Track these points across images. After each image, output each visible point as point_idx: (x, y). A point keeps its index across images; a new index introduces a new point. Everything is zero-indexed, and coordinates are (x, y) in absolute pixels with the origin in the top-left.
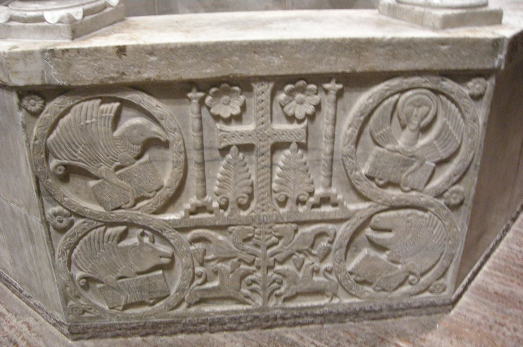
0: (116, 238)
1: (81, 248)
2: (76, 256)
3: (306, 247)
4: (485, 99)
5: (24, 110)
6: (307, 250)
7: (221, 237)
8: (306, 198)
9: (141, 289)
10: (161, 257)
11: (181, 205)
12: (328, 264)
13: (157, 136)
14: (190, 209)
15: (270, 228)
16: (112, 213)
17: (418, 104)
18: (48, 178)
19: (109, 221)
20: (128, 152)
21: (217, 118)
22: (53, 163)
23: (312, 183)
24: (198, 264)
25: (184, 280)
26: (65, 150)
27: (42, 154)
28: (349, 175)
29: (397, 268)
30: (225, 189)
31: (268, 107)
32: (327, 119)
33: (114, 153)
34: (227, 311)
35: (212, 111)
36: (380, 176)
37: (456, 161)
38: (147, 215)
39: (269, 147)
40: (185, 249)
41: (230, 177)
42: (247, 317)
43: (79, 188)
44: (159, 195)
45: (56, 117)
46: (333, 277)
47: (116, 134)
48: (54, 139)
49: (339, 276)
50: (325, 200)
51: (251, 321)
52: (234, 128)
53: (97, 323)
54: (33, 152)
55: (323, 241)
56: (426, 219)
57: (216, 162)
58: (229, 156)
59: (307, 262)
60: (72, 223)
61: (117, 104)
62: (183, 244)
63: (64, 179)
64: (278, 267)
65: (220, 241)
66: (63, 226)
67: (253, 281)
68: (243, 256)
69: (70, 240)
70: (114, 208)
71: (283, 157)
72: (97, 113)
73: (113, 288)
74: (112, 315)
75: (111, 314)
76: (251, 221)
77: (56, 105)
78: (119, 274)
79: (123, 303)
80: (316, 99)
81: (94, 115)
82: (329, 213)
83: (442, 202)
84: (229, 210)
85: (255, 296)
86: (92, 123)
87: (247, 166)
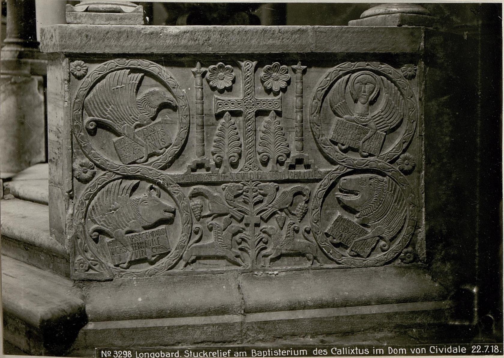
0: (129, 191)
1: (98, 199)
2: (93, 207)
3: (287, 206)
6: (287, 208)
10: (165, 211)
13: (169, 101)
16: (129, 167)
17: (365, 82)
18: (81, 132)
19: (126, 174)
21: (213, 89)
26: (98, 109)
28: (317, 139)
29: (367, 233)
35: (211, 83)
36: (342, 141)
39: (254, 113)
40: (186, 203)
43: (104, 144)
47: (139, 97)
50: (299, 161)
54: (73, 108)
58: (222, 121)
59: (288, 222)
61: (142, 74)
64: (263, 226)
66: (86, 177)
69: (90, 191)
71: (264, 123)
78: (127, 229)
79: (128, 260)
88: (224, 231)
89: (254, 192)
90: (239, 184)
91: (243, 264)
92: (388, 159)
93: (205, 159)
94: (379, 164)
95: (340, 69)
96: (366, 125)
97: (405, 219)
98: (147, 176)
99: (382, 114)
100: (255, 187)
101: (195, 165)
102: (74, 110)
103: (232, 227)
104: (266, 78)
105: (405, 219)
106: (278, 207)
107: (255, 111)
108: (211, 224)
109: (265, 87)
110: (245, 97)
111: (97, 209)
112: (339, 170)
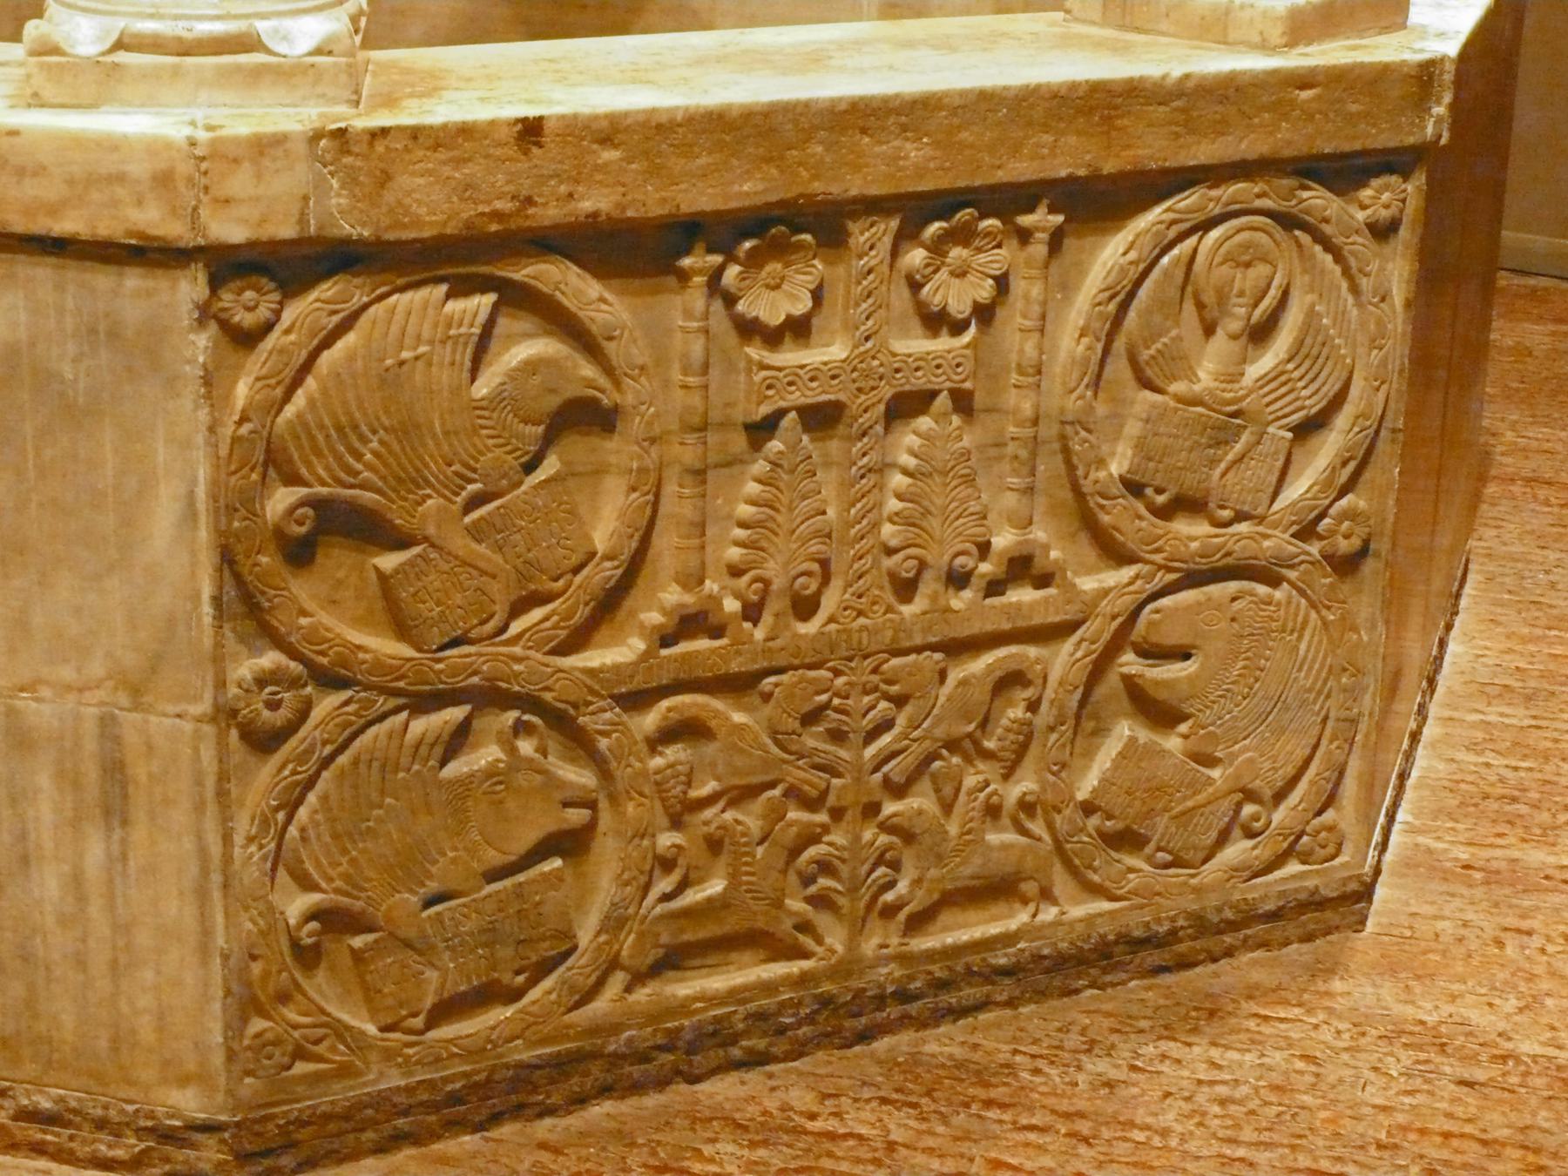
0: (439, 751)
1: (324, 798)
2: (303, 830)
4: (1404, 232)
5: (213, 327)
6: (970, 735)
7: (738, 717)
8: (971, 564)
9: (490, 935)
10: (566, 805)
11: (632, 614)
12: (1024, 785)
14: (662, 625)
15: (875, 671)
16: (439, 661)
17: (1246, 258)
19: (427, 688)
20: (509, 448)
21: (748, 329)
22: (280, 500)
24: (665, 822)
25: (627, 883)
27: (252, 469)
28: (1082, 482)
29: (1210, 781)
30: (762, 549)
33: (465, 450)
34: (745, 988)
35: (741, 307)
37: (1342, 420)
38: (539, 656)
39: (882, 407)
41: (777, 510)
42: (800, 1004)
44: (579, 587)
45: (315, 342)
46: (1037, 827)
47: (481, 389)
48: (299, 415)
49: (1058, 819)
50: (1022, 568)
51: (810, 1019)
52: (790, 356)
53: (339, 1095)
56: (1279, 604)
57: (736, 469)
58: (775, 445)
59: (970, 781)
60: (303, 714)
63: (299, 553)
64: (890, 808)
65: (741, 728)
66: (279, 723)
67: (825, 867)
68: (802, 774)
69: (294, 772)
70: (446, 640)
71: (911, 440)
72: (436, 325)
73: (408, 944)
74: (389, 1055)
75: (386, 1049)
76: (827, 652)
77: (318, 305)
78: (433, 886)
79: (429, 1001)
80: (998, 258)
81: (426, 334)
82: (1033, 605)
83: (1314, 549)
84: (767, 618)
85: (823, 920)
86: (417, 358)
88: (761, 843)
91: (819, 950)
92: (1293, 523)
94: (1266, 543)
95: (1172, 216)
96: (1234, 415)
97: (1326, 718)
98: (504, 685)
99: (1290, 366)
102: (233, 468)
103: (790, 824)
104: (931, 269)
105: (1326, 718)
107: (889, 395)
108: (718, 828)
110: (856, 347)
111: (319, 836)
112: (1139, 582)
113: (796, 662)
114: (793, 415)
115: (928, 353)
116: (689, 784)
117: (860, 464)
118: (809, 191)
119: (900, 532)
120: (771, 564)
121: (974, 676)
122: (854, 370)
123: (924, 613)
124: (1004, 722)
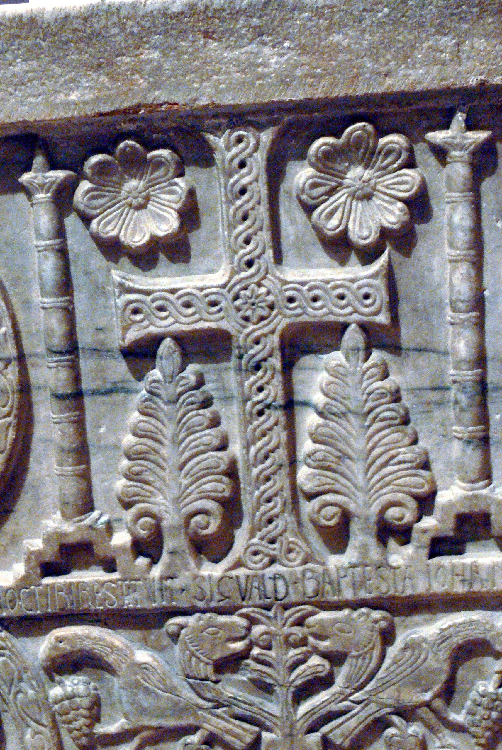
6: (428, 705)
8: (408, 517)
11: (15, 540)
14: (39, 553)
15: (300, 622)
23: (426, 466)
31: (263, 211)
32: (451, 246)
35: (94, 224)
39: (276, 339)
40: (31, 692)
55: (482, 675)
57: (119, 397)
62: (25, 676)
65: (143, 667)
71: (323, 377)
84: (165, 557)
87: (216, 407)
89: (295, 646)
90: (235, 619)
93: (91, 527)
100: (295, 629)
101: (56, 548)
104: (322, 190)
106: (390, 702)
107: (280, 328)
109: (318, 230)
110: (234, 273)
113: (201, 605)
114: (168, 342)
115: (328, 282)
116: (97, 718)
117: (256, 399)
118: (150, 100)
119: (314, 475)
120: (160, 498)
121: (425, 640)
122: (236, 297)
123: (353, 566)
124: (473, 694)
